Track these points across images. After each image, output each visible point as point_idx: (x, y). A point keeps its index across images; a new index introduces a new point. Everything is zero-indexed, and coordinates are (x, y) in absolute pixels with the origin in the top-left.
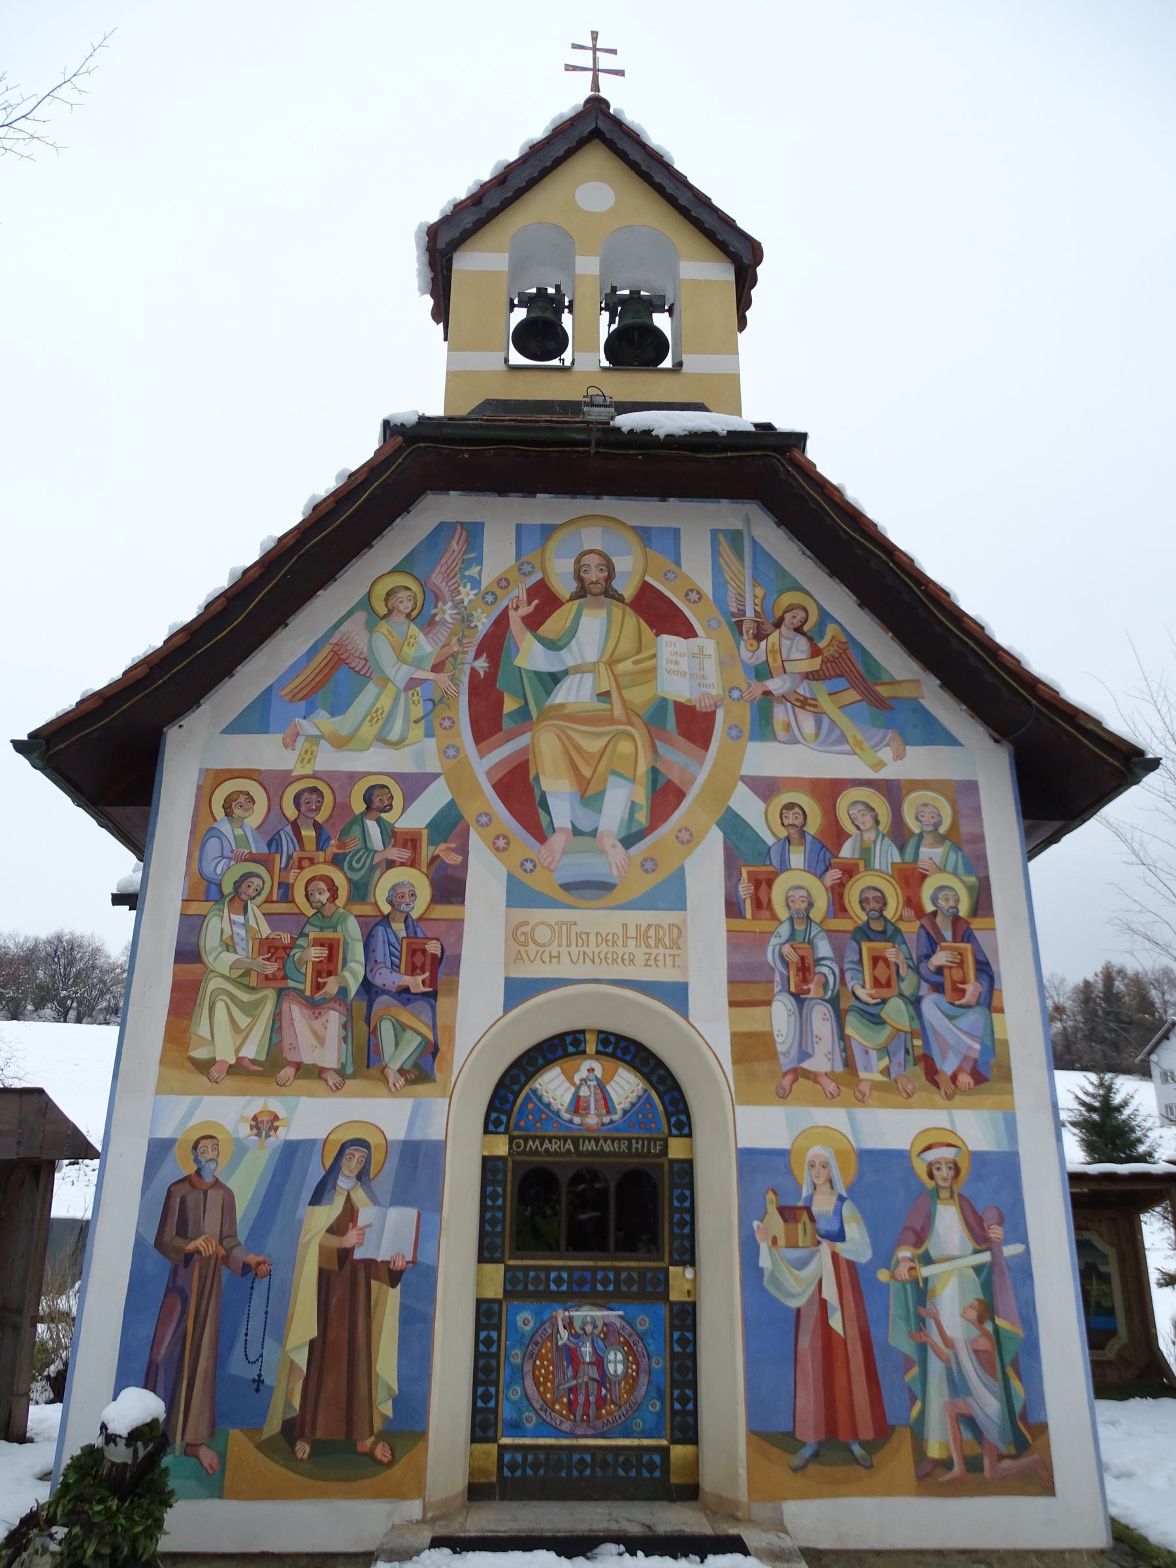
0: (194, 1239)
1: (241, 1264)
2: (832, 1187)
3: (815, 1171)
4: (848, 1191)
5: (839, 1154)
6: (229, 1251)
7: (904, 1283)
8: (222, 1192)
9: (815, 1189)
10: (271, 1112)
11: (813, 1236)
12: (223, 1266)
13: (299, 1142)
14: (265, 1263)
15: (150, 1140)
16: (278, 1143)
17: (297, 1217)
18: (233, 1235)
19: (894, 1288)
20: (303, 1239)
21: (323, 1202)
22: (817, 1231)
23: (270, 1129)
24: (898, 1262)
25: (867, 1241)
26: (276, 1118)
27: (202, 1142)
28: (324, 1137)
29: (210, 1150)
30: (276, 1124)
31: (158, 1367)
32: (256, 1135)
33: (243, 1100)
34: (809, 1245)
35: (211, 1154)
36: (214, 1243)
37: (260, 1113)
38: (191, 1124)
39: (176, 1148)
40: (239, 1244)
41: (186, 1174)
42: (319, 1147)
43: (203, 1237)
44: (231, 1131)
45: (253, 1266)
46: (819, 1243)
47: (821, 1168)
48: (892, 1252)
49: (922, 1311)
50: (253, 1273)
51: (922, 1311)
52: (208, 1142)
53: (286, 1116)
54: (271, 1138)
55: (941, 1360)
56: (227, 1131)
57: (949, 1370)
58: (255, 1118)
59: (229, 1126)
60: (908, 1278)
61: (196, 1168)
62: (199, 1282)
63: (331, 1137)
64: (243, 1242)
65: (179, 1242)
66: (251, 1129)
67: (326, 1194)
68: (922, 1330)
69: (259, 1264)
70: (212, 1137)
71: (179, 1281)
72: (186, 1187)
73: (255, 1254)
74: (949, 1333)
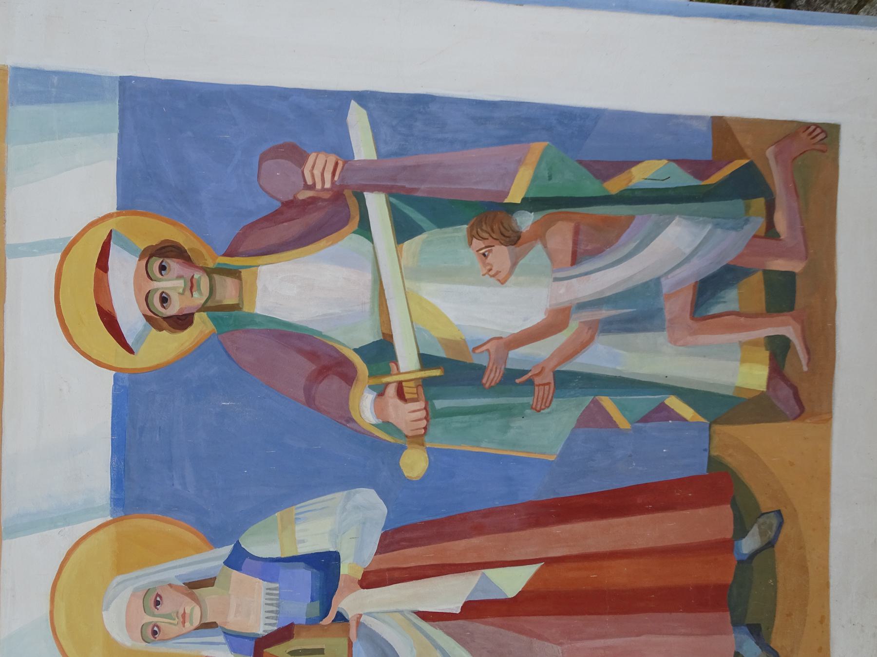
2: (208, 582)
3: (169, 627)
4: (215, 543)
5: (122, 566)
7: (430, 414)
9: (212, 625)
11: (325, 630)
19: (439, 440)
22: (313, 622)
24: (386, 425)
25: (339, 497)
34: (345, 642)
46: (341, 618)
47: (163, 609)
48: (361, 435)
49: (491, 377)
51: (491, 377)
55: (591, 340)
57: (611, 326)
60: (421, 405)
68: (530, 382)
74: (536, 317)
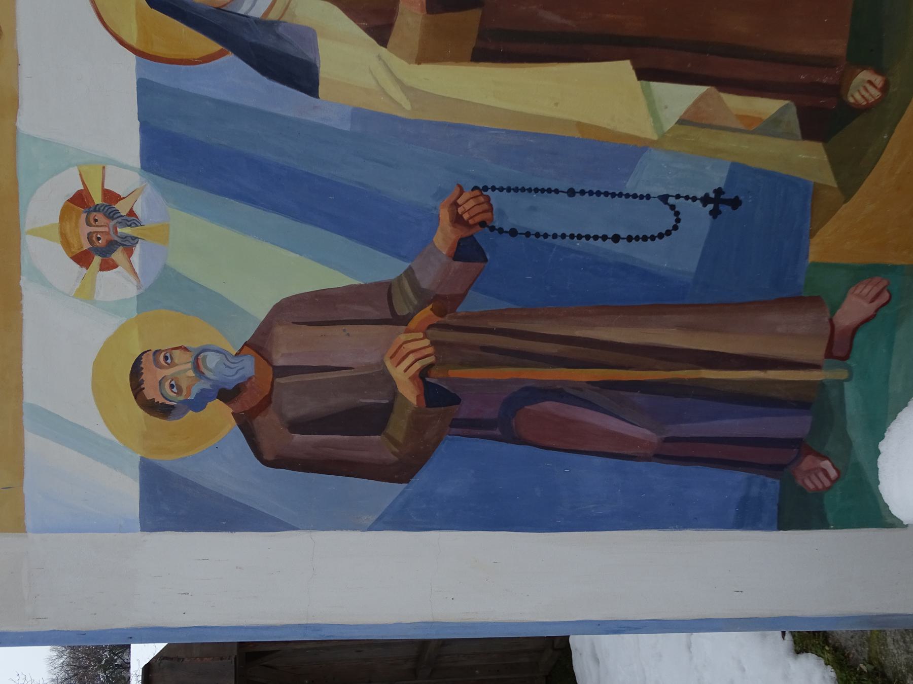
0: (395, 387)
1: (457, 264)
6: (424, 298)
8: (279, 330)
10: (65, 214)
12: (461, 310)
13: (145, 129)
14: (455, 205)
15: (145, 528)
16: (149, 189)
17: (347, 127)
18: (387, 290)
20: (404, 107)
21: (311, 56)
23: (112, 214)
26: (80, 199)
27: (151, 393)
28: (132, 57)
29: (169, 372)
30: (98, 199)
31: (667, 440)
32: (129, 252)
33: (30, 292)
35: (183, 368)
36: (403, 337)
37: (66, 244)
38: (103, 431)
39: (163, 459)
40: (409, 273)
41: (232, 423)
42: (160, 74)
43: (389, 364)
44: (123, 320)
45: (464, 233)
50: (482, 237)
52: (151, 378)
53: (75, 171)
54: (138, 210)
56: (122, 331)
58: (82, 259)
59: (111, 324)
61: (217, 402)
62: (501, 365)
63: (133, 41)
64: (405, 265)
65: (398, 426)
66: (115, 266)
67: (290, 50)
69: (457, 220)
70: (136, 372)
71: (491, 412)
72: (268, 423)
73: (433, 231)
